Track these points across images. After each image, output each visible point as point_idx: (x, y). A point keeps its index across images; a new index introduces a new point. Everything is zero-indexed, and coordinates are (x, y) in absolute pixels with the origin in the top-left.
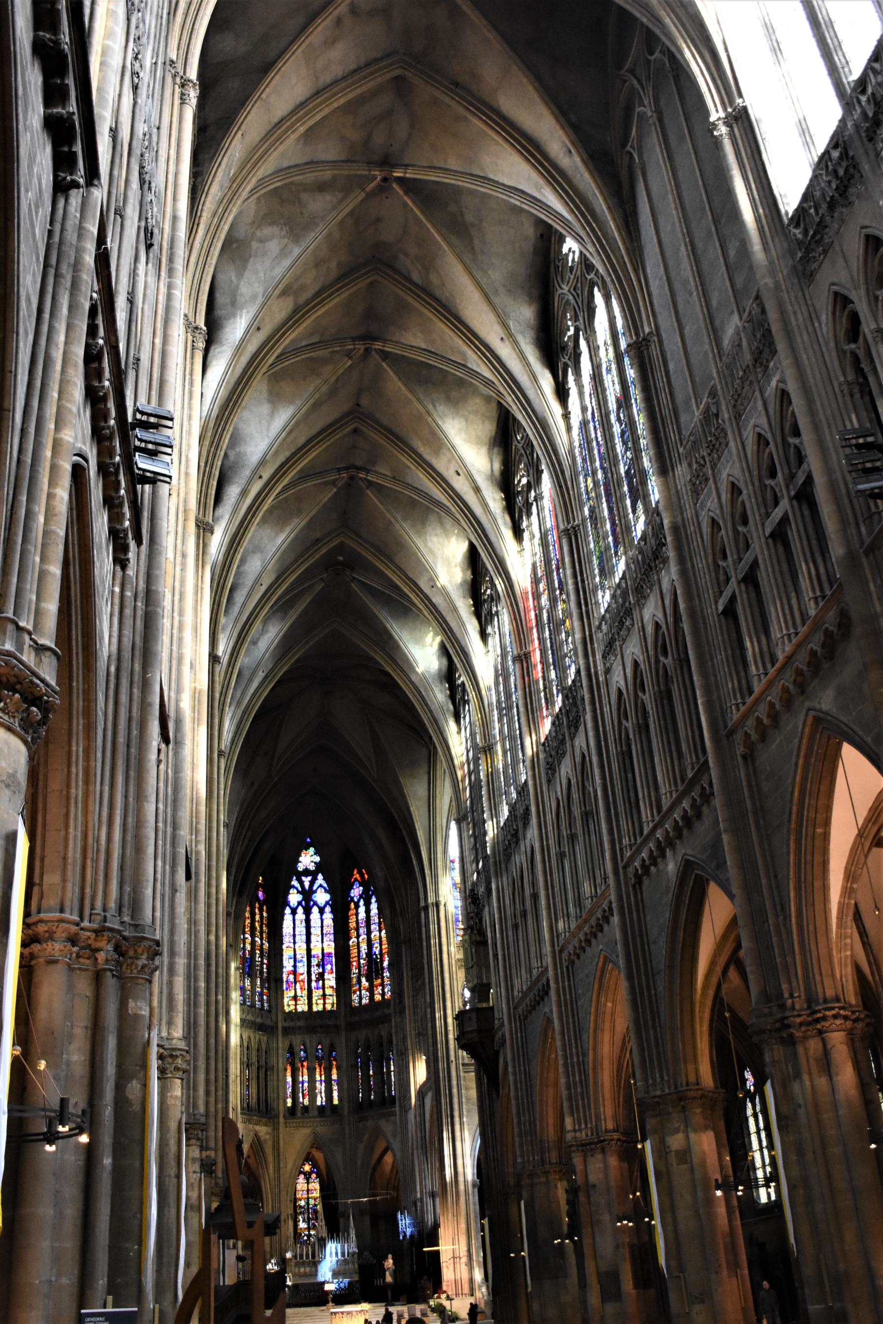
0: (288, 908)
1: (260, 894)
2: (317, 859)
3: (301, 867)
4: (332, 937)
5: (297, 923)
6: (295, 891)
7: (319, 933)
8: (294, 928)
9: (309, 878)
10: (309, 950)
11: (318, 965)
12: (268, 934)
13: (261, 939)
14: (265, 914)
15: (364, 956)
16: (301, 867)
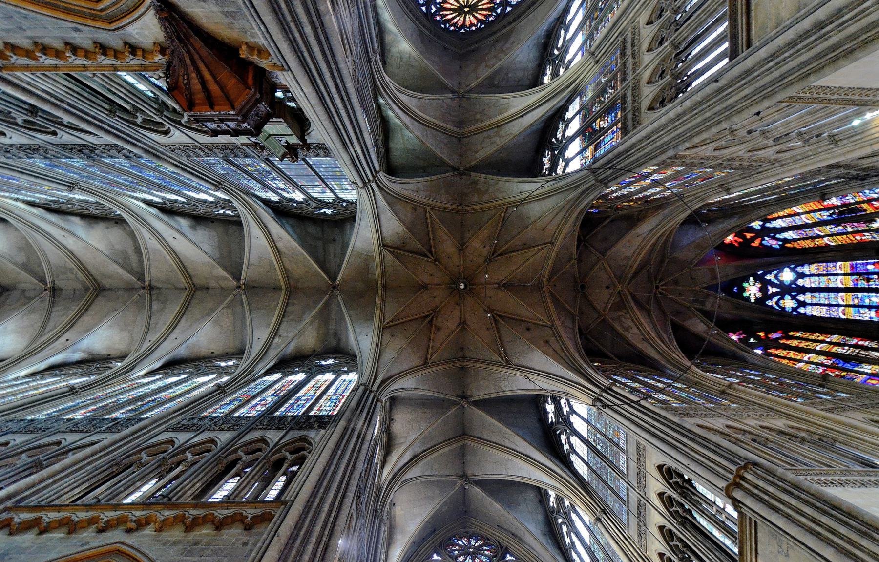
0: (799, 310)
1: (774, 336)
2: (751, 279)
3: (759, 295)
4: (831, 265)
5: (815, 301)
6: (781, 301)
7: (826, 278)
8: (821, 305)
9: (769, 287)
10: (847, 290)
11: (868, 280)
12: (821, 333)
13: (823, 342)
14: (799, 334)
15: (841, 228)
16: (759, 295)
